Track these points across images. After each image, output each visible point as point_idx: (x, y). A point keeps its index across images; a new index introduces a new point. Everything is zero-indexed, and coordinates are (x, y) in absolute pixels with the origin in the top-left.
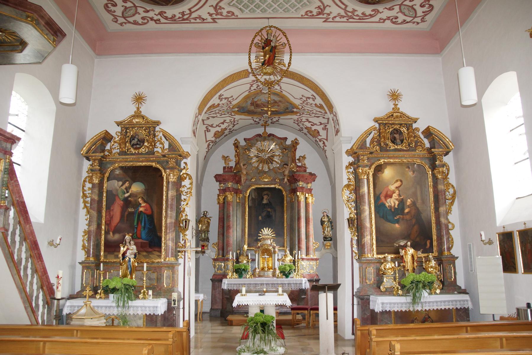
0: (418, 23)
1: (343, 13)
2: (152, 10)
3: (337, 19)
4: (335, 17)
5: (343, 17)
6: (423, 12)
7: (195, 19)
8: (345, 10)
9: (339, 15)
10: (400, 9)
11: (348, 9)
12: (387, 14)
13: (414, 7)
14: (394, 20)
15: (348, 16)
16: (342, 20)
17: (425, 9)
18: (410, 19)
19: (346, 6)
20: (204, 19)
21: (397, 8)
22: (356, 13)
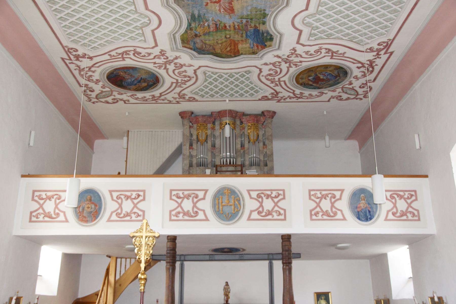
0: (361, 99)
1: (292, 95)
2: (125, 93)
3: (288, 100)
4: (286, 98)
5: (293, 98)
6: (364, 92)
7: (163, 100)
8: (294, 93)
9: (289, 96)
10: (342, 90)
11: (295, 92)
12: (330, 94)
13: (355, 88)
14: (339, 98)
15: (297, 97)
16: (293, 100)
17: (365, 89)
18: (355, 96)
19: (294, 91)
20: (171, 101)
21: (340, 90)
22: (304, 95)
